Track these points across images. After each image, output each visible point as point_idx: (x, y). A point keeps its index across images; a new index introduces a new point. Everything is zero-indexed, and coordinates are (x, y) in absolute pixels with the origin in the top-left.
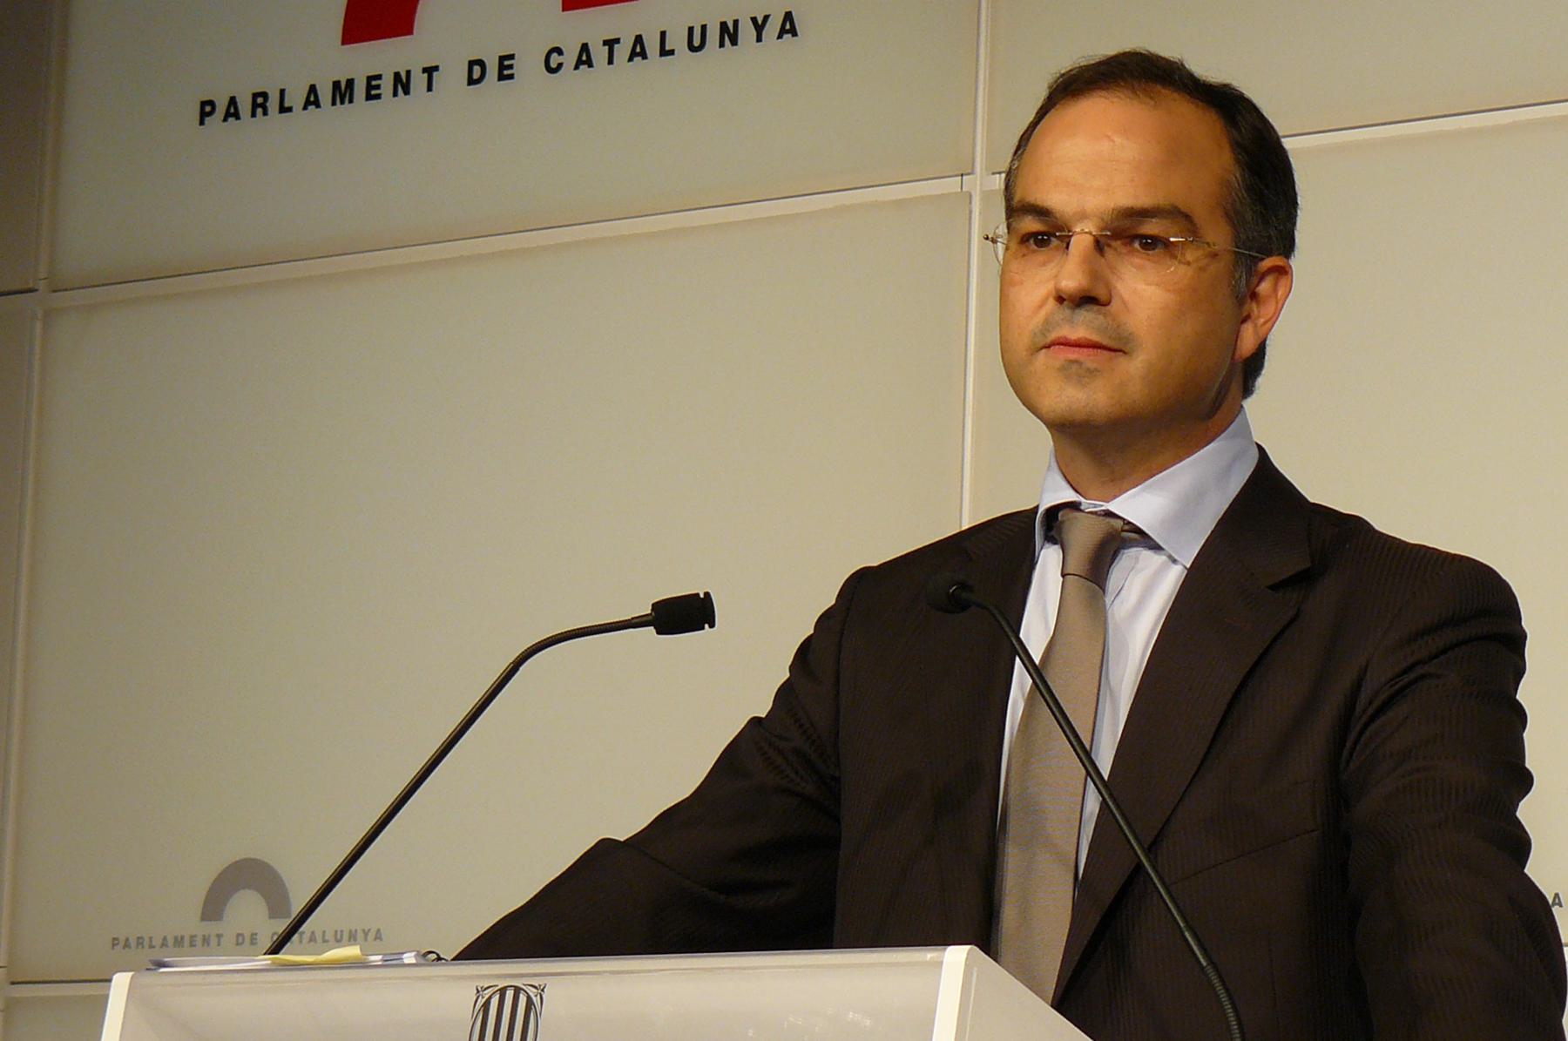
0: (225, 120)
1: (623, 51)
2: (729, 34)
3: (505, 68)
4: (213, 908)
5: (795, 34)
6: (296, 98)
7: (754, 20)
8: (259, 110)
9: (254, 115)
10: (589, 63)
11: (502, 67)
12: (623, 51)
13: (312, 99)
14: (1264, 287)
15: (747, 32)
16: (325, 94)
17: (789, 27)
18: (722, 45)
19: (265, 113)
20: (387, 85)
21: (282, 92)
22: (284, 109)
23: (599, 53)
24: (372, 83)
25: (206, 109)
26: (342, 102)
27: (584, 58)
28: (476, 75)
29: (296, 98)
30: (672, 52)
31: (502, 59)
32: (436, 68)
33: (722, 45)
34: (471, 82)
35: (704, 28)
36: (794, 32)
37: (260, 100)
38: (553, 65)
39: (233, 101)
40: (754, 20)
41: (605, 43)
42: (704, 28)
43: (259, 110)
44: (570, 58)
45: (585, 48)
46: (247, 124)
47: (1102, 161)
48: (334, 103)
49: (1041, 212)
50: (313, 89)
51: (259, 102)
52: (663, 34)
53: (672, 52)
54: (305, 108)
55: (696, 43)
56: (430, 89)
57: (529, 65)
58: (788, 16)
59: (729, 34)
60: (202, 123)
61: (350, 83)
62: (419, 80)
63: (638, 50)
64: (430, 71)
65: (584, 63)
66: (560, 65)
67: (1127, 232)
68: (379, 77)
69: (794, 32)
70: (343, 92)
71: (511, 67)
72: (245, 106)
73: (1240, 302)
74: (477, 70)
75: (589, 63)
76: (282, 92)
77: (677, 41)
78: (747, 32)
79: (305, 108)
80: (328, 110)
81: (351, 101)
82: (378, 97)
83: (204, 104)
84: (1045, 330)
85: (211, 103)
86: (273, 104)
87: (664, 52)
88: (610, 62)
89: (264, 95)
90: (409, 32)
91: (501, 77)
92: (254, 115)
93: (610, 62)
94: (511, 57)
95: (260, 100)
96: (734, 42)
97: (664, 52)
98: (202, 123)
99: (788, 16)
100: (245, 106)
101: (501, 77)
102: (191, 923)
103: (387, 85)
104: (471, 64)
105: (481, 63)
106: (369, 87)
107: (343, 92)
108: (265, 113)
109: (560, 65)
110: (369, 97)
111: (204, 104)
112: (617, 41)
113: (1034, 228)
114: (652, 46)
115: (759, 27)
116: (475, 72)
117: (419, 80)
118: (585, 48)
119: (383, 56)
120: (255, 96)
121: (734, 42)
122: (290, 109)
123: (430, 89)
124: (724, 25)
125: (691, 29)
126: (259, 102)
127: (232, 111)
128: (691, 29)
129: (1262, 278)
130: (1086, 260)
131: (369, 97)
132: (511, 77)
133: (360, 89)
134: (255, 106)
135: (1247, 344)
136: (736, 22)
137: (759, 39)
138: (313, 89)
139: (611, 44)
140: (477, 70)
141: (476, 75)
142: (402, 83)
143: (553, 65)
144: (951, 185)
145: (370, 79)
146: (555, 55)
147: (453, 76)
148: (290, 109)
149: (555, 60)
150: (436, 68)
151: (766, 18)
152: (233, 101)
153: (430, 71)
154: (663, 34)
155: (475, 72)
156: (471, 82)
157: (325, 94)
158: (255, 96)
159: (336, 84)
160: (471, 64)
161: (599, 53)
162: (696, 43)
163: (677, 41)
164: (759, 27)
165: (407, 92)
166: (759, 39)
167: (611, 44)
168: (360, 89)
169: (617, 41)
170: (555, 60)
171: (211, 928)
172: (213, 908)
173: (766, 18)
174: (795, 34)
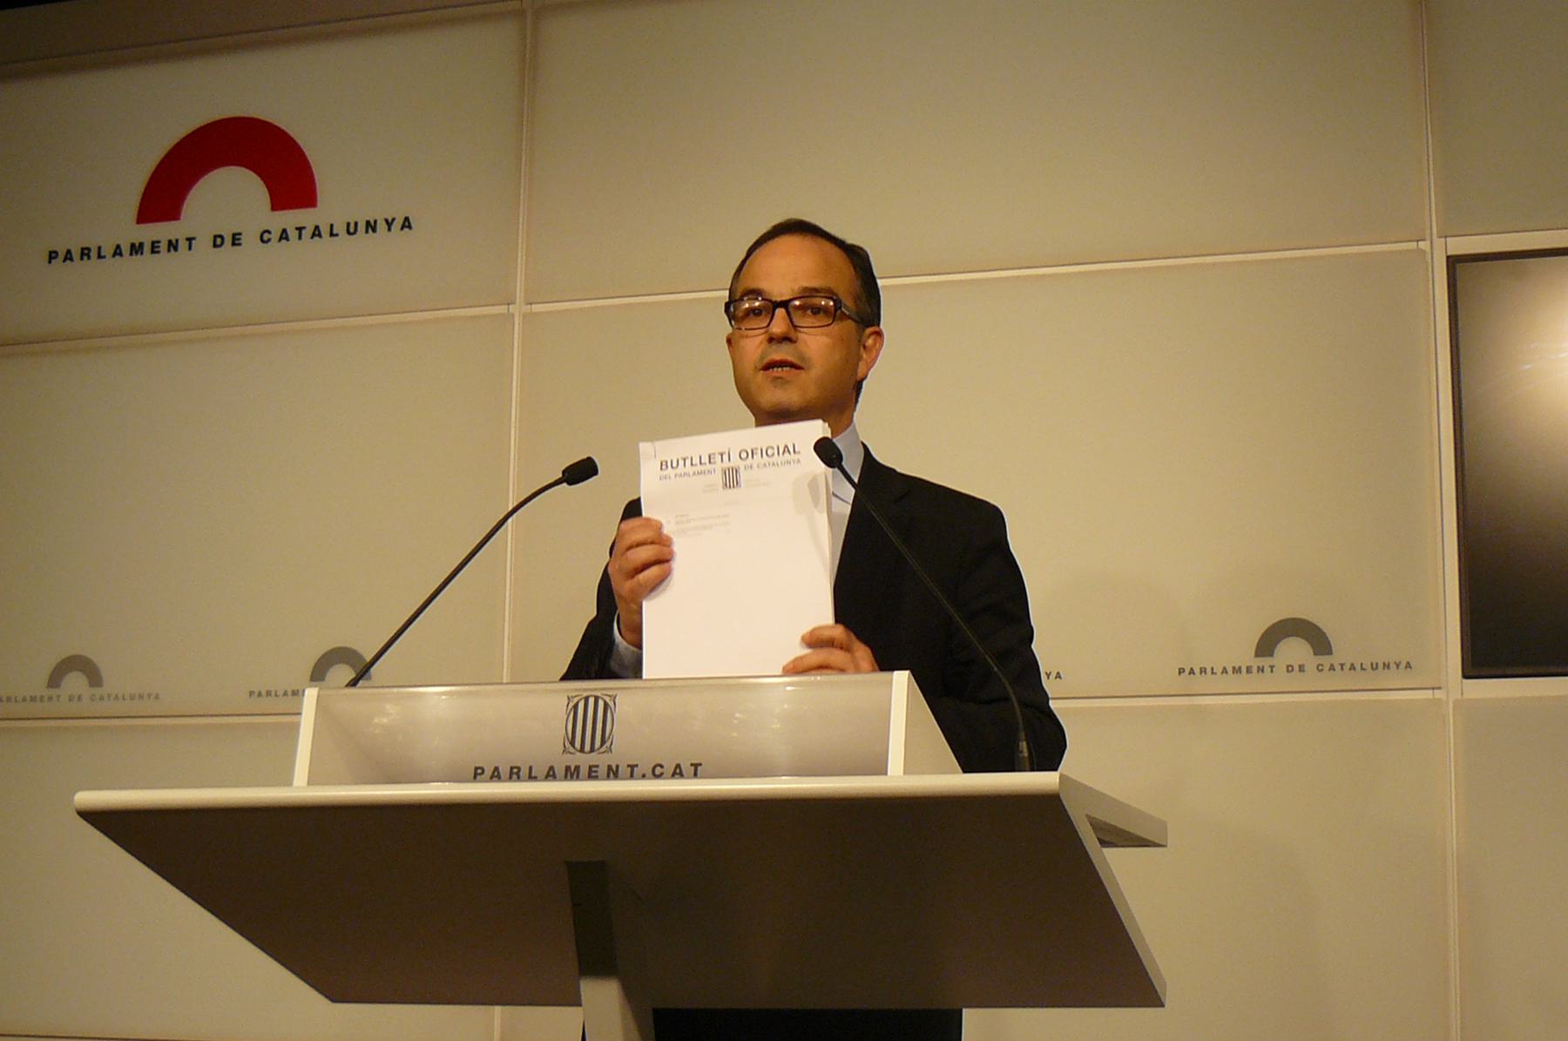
2: (371, 226)
3: (236, 240)
4: (55, 680)
6: (108, 250)
10: (287, 239)
12: (307, 234)
13: (118, 252)
14: (870, 342)
15: (382, 226)
16: (126, 249)
17: (407, 224)
20: (163, 246)
22: (100, 256)
23: (293, 234)
25: (53, 255)
27: (284, 236)
29: (108, 250)
34: (215, 246)
36: (410, 227)
39: (69, 252)
44: (275, 235)
45: (284, 231)
47: (788, 271)
50: (118, 247)
51: (85, 253)
58: (407, 219)
59: (371, 226)
61: (141, 245)
62: (183, 245)
63: (317, 233)
64: (190, 240)
67: (809, 303)
69: (410, 227)
70: (136, 249)
72: (76, 254)
75: (287, 239)
77: (340, 229)
78: (382, 226)
80: (128, 261)
84: (762, 358)
86: (94, 254)
87: (332, 235)
96: (374, 230)
97: (332, 235)
99: (407, 219)
100: (76, 254)
102: (39, 686)
103: (163, 246)
107: (136, 249)
114: (325, 231)
115: (389, 224)
116: (218, 241)
117: (183, 245)
118: (284, 231)
119: (161, 231)
124: (368, 223)
126: (85, 253)
127: (68, 256)
133: (147, 248)
134: (82, 254)
138: (118, 247)
142: (173, 246)
144: (503, 309)
147: (203, 242)
149: (266, 236)
152: (69, 252)
153: (190, 240)
155: (218, 241)
156: (215, 246)
157: (126, 249)
159: (133, 245)
161: (293, 234)
163: (340, 229)
164: (389, 224)
167: (300, 229)
168: (147, 248)
170: (266, 236)
171: (53, 692)
172: (55, 680)
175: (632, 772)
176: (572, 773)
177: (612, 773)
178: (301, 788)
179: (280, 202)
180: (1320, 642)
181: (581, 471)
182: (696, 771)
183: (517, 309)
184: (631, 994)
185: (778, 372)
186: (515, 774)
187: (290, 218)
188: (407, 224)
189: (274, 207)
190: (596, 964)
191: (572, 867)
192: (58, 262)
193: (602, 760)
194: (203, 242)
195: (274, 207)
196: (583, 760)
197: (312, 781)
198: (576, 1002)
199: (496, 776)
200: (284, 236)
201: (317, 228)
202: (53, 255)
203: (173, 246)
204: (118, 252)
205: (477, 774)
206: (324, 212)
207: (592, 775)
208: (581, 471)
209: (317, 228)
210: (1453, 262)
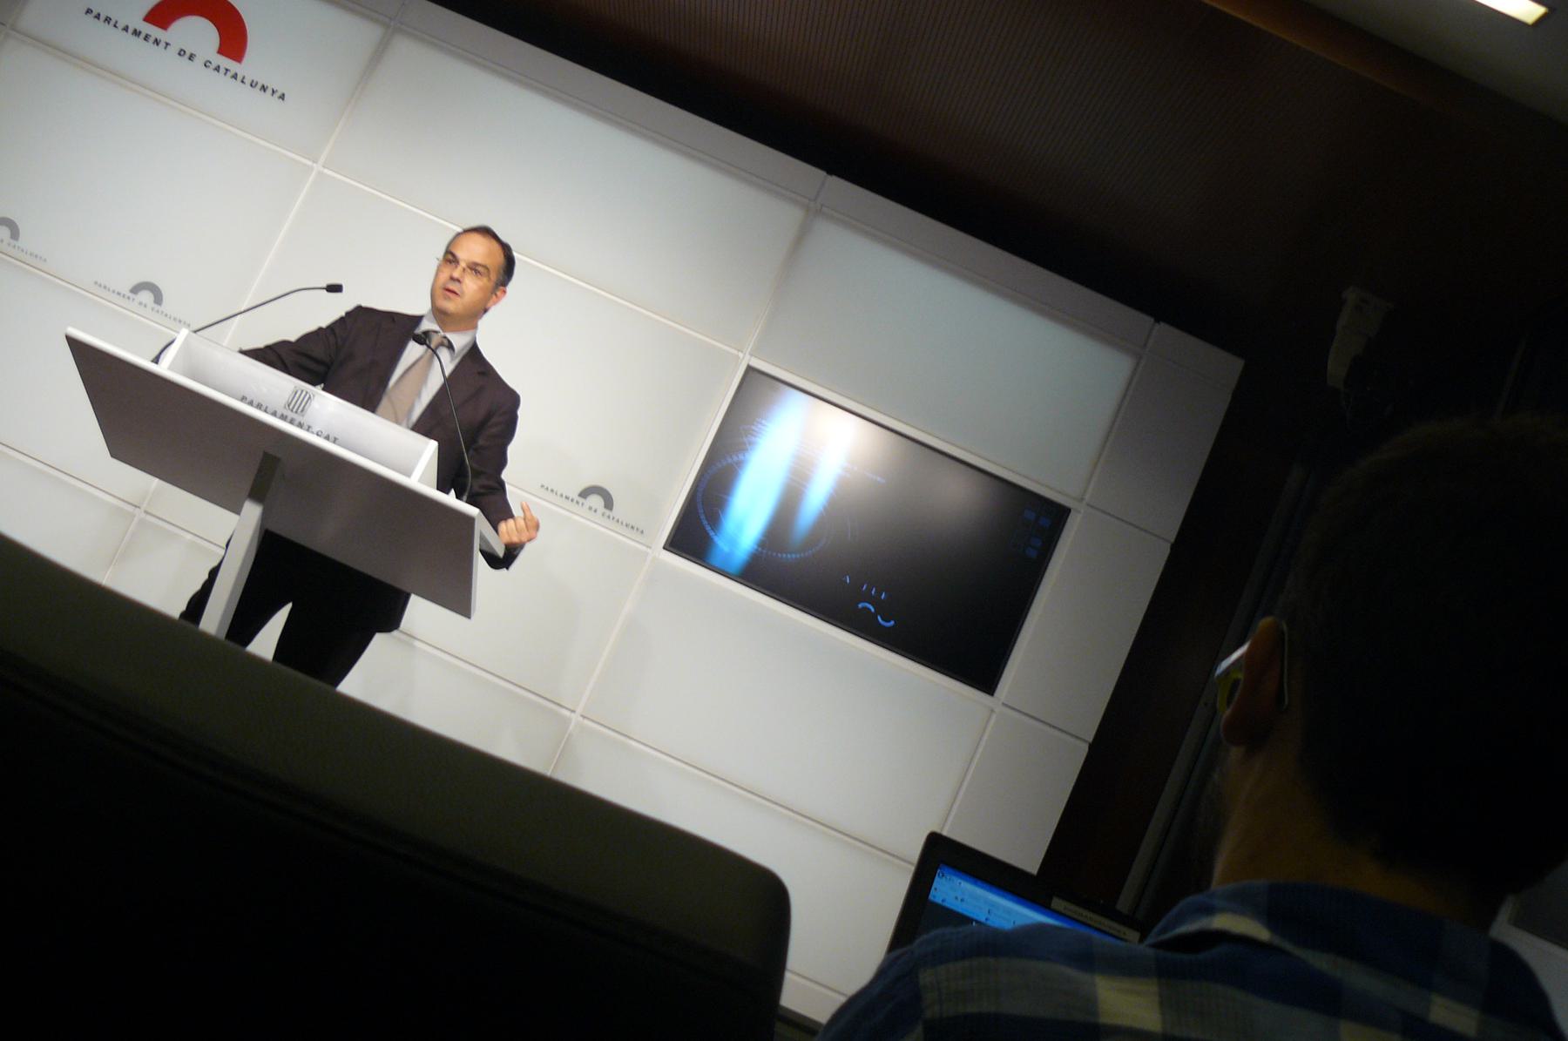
2: (264, 88)
3: (191, 57)
6: (121, 25)
13: (126, 29)
17: (282, 97)
23: (222, 70)
44: (214, 65)
46: (100, 24)
51: (108, 20)
57: (199, 61)
59: (264, 88)
63: (235, 76)
70: (136, 33)
72: (102, 18)
77: (248, 81)
78: (269, 91)
107: (136, 33)
117: (162, 45)
119: (155, 31)
126: (108, 20)
127: (98, 17)
142: (157, 42)
147: (173, 50)
155: (181, 53)
161: (222, 70)
175: (308, 429)
176: (283, 418)
177: (300, 425)
178: (163, 369)
179: (222, 51)
180: (609, 503)
181: (335, 289)
182: (335, 441)
183: (317, 167)
184: (265, 517)
186: (259, 406)
187: (225, 62)
188: (282, 97)
189: (221, 52)
190: (257, 495)
191: (265, 454)
192: (90, 16)
193: (298, 418)
194: (173, 50)
195: (221, 52)
196: (290, 415)
197: (170, 368)
198: (238, 512)
199: (251, 403)
200: (217, 69)
202: (89, 11)
203: (157, 42)
204: (126, 29)
205: (243, 399)
207: (292, 422)
208: (335, 289)
210: (750, 369)
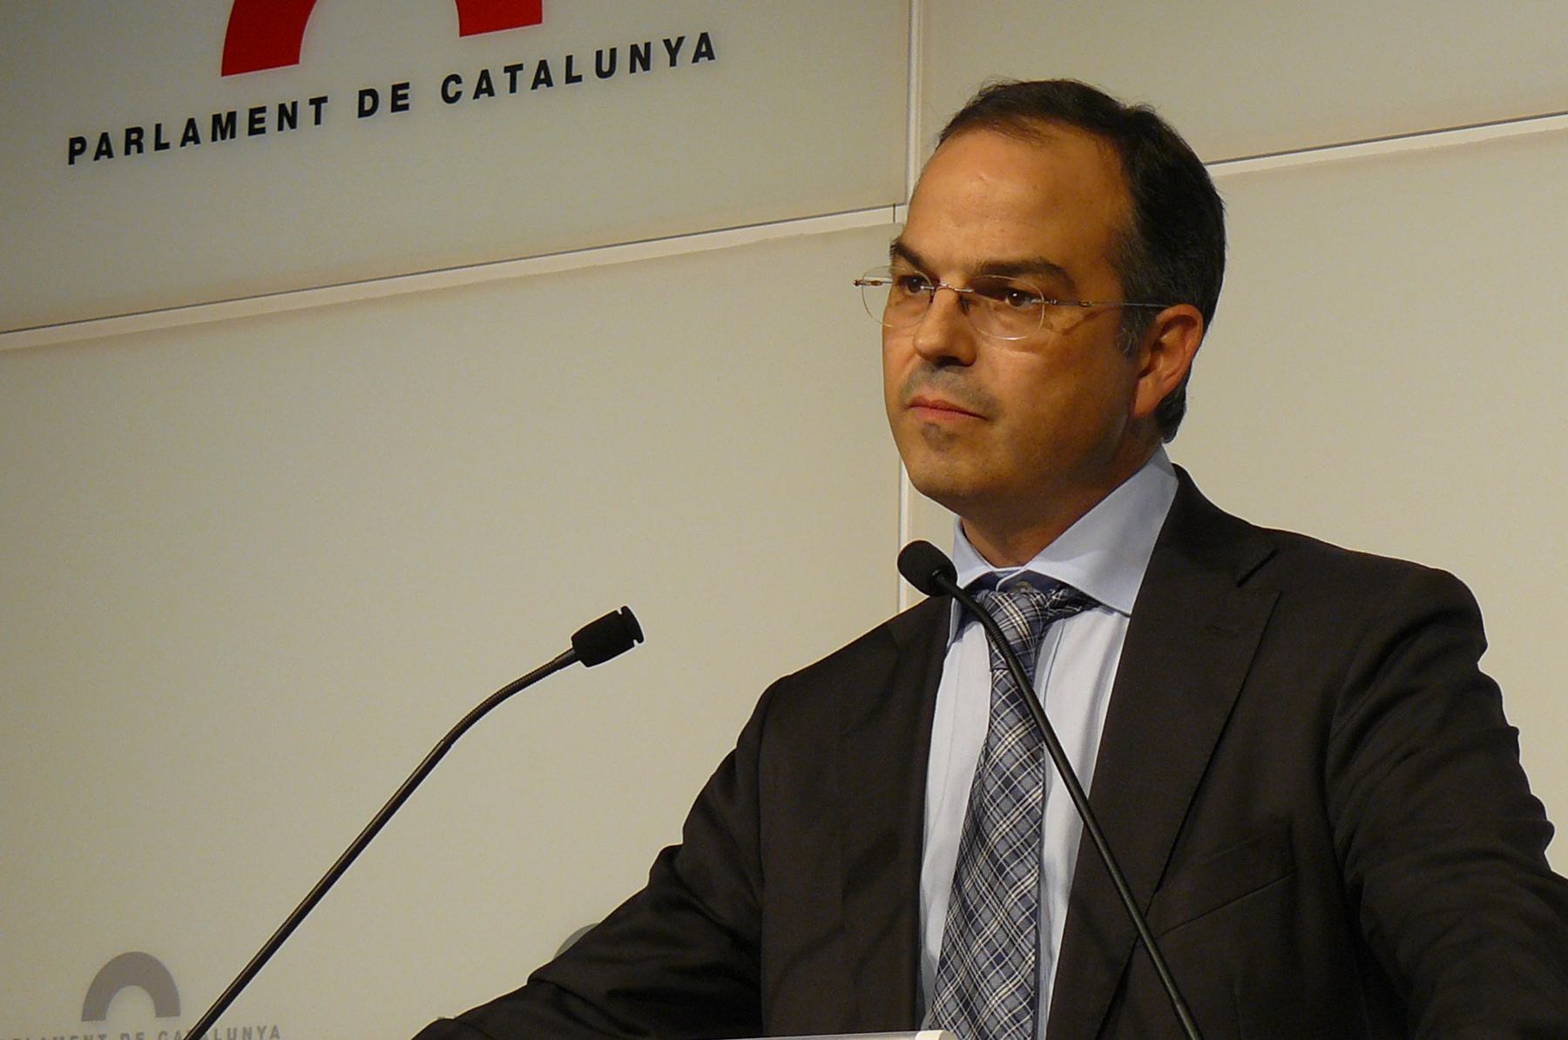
0: (96, 158)
1: (526, 77)
2: (640, 58)
5: (711, 57)
6: (173, 134)
7: (667, 42)
8: (134, 148)
9: (127, 152)
11: (395, 97)
12: (526, 77)
13: (191, 134)
15: (660, 55)
16: (205, 128)
17: (705, 49)
18: (633, 70)
19: (140, 150)
20: (271, 118)
21: (158, 127)
22: (160, 146)
23: (500, 81)
24: (256, 116)
25: (76, 147)
26: (223, 138)
27: (485, 86)
28: (368, 106)
29: (173, 134)
30: (579, 79)
31: (395, 88)
32: (324, 99)
33: (633, 70)
34: (363, 113)
35: (613, 51)
37: (134, 136)
38: (451, 94)
39: (104, 138)
40: (667, 42)
41: (507, 69)
42: (613, 51)
43: (134, 148)
45: (485, 75)
48: (214, 139)
49: (915, 260)
50: (191, 123)
51: (134, 138)
52: (569, 59)
53: (579, 79)
54: (183, 144)
55: (606, 68)
56: (318, 121)
57: (424, 95)
58: (704, 38)
59: (640, 58)
60: (71, 162)
62: (306, 113)
63: (543, 76)
64: (318, 102)
65: (104, 153)
66: (458, 94)
68: (262, 110)
70: (224, 126)
71: (405, 97)
72: (118, 143)
73: (1132, 354)
74: (368, 100)
76: (158, 127)
77: (586, 66)
78: (660, 55)
79: (183, 144)
80: (209, 150)
81: (233, 136)
82: (262, 131)
83: (73, 141)
85: (81, 140)
86: (149, 140)
87: (571, 79)
88: (513, 90)
89: (139, 131)
90: (294, 59)
91: (395, 108)
92: (127, 152)
93: (513, 90)
94: (406, 86)
95: (134, 136)
97: (571, 79)
98: (71, 162)
99: (704, 38)
100: (118, 143)
101: (395, 108)
103: (271, 118)
104: (362, 94)
105: (373, 93)
106: (253, 121)
107: (224, 126)
108: (140, 150)
109: (458, 94)
110: (252, 132)
111: (73, 141)
112: (520, 67)
113: (913, 275)
114: (558, 73)
115: (673, 50)
116: (367, 101)
117: (306, 113)
118: (485, 75)
119: (267, 87)
120: (129, 132)
121: (646, 67)
122: (166, 146)
123: (318, 121)
124: (634, 48)
125: (599, 54)
127: (104, 149)
128: (599, 54)
129: (1167, 326)
130: (947, 317)
131: (252, 132)
132: (406, 107)
134: (129, 143)
135: (1148, 393)
136: (647, 45)
137: (673, 63)
138: (191, 123)
139: (513, 70)
140: (368, 100)
141: (368, 106)
142: (288, 116)
143: (451, 94)
145: (253, 112)
146: (453, 83)
147: (343, 106)
148: (166, 146)
149: (452, 88)
150: (324, 99)
151: (680, 40)
152: (104, 138)
153: (318, 102)
154: (569, 59)
155: (367, 101)
156: (363, 113)
157: (205, 128)
158: (129, 132)
159: (217, 118)
160: (362, 94)
161: (500, 81)
162: (606, 68)
163: (586, 66)
164: (673, 50)
165: (293, 125)
166: (673, 63)
167: (513, 70)
169: (520, 67)
170: (452, 88)
173: (680, 40)
174: (711, 57)
185: (931, 417)
187: (498, 48)
200: (485, 86)
201: (543, 65)
204: (191, 134)
206: (567, 27)
209: (543, 65)
